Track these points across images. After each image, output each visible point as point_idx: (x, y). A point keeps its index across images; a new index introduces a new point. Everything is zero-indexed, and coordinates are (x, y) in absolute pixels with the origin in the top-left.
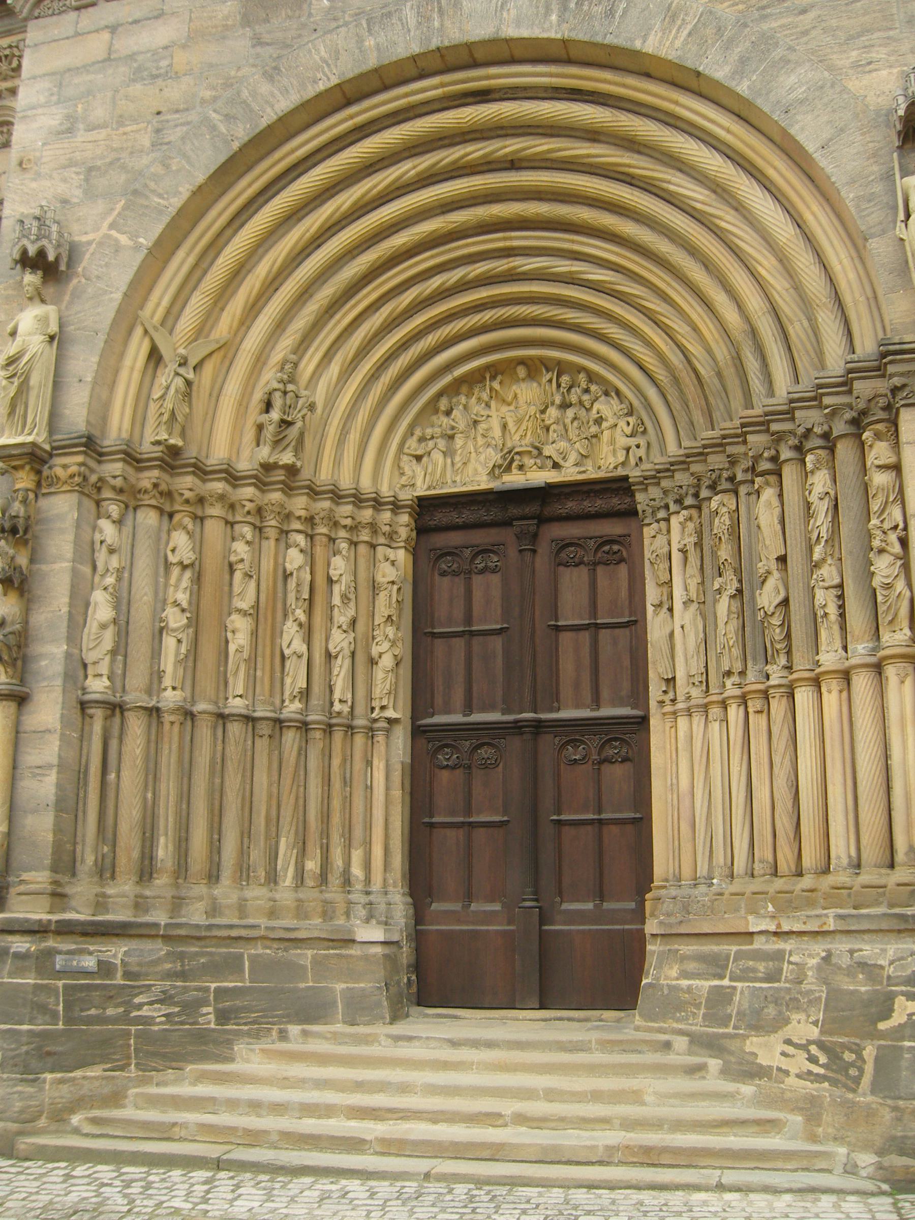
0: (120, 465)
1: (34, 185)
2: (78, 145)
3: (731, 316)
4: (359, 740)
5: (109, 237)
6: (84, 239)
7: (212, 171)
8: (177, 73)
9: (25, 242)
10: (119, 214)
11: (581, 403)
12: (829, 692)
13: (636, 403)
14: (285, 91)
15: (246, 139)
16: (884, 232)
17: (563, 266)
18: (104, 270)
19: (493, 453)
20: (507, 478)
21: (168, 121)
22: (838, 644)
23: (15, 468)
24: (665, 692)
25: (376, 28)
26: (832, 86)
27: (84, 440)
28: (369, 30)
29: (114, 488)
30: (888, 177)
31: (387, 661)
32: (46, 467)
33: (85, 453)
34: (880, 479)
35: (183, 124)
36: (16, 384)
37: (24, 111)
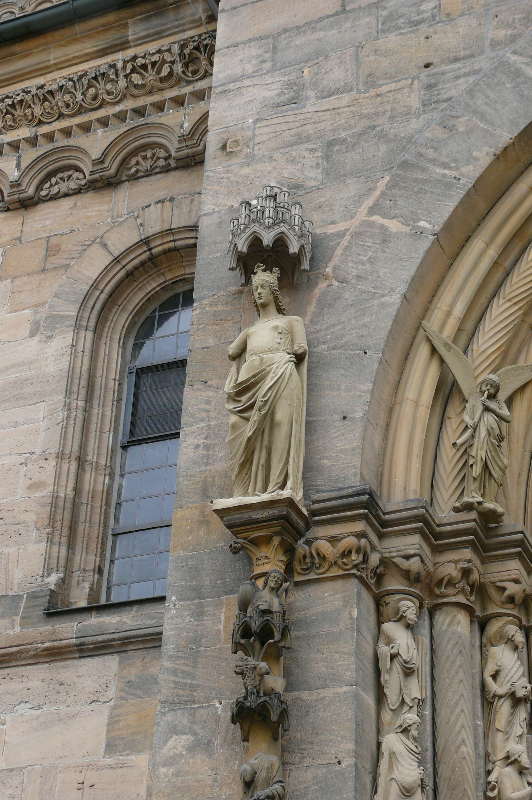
0: (416, 539)
1: (246, 171)
2: (308, 116)
5: (371, 224)
6: (331, 230)
7: (522, 127)
8: (448, 15)
9: (255, 228)
10: (383, 194)
18: (368, 266)
21: (443, 73)
23: (255, 542)
27: (366, 497)
29: (406, 574)
32: (301, 542)
33: (365, 517)
36: (256, 418)
37: (223, 85)
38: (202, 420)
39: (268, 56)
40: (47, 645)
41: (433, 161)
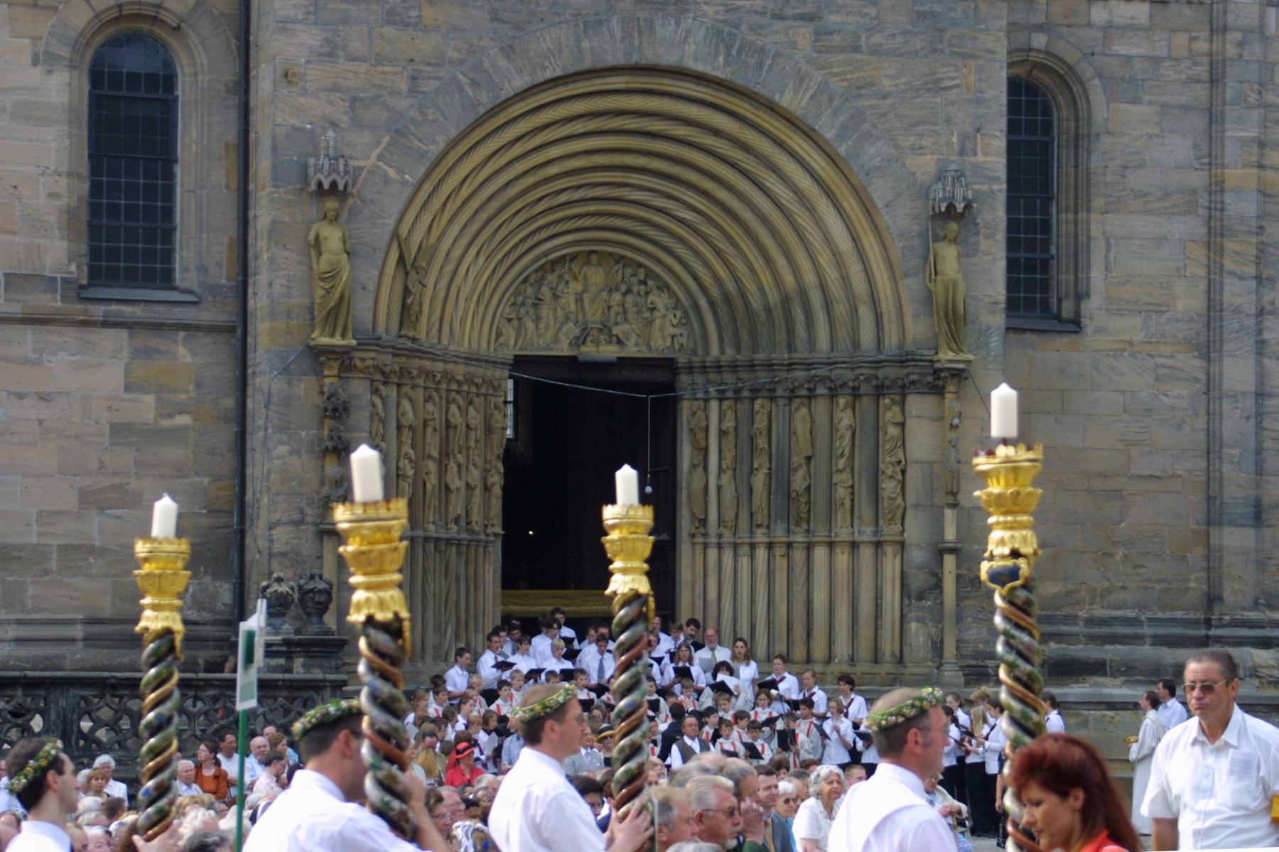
1: (302, 100)
3: (788, 279)
4: (481, 550)
5: (378, 167)
8: (425, 26)
10: (385, 149)
11: (638, 293)
12: (843, 553)
13: (685, 302)
14: (520, 71)
15: (490, 106)
16: (916, 274)
17: (661, 202)
19: (573, 327)
20: (583, 349)
21: (421, 72)
22: (849, 523)
23: (329, 359)
24: (697, 528)
25: (591, 32)
26: (897, 161)
28: (585, 33)
30: (923, 235)
31: (497, 490)
34: (893, 431)
35: (435, 78)
38: (284, 270)
39: (312, 9)
40: (82, 318)
41: (414, 135)
